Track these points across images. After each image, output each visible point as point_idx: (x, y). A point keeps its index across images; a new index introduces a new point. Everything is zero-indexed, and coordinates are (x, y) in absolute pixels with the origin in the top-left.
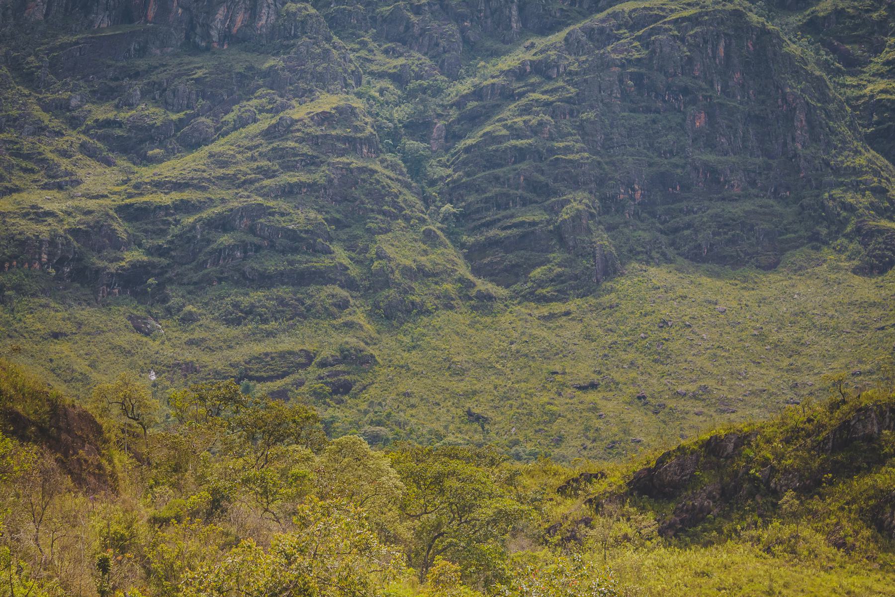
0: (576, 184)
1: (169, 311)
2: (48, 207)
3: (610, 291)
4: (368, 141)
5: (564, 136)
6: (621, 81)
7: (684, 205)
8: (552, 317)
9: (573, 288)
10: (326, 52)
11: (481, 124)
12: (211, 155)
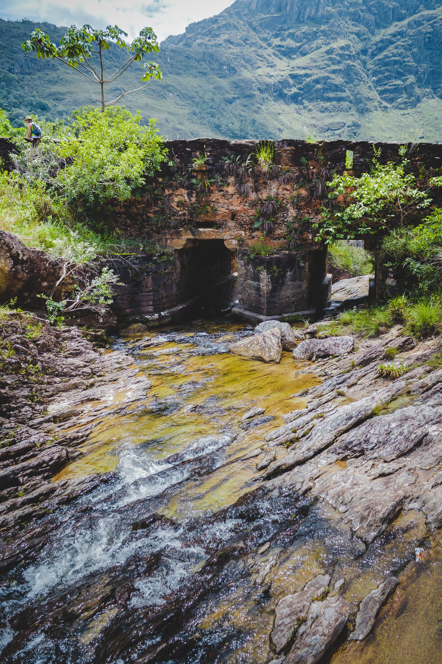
0: (410, 73)
1: (304, 107)
2: (272, 74)
3: (419, 107)
4: (354, 56)
5: (407, 57)
6: (424, 39)
7: (438, 80)
8: (404, 114)
9: (410, 106)
10: (339, 25)
11: (383, 51)
12: (311, 59)
